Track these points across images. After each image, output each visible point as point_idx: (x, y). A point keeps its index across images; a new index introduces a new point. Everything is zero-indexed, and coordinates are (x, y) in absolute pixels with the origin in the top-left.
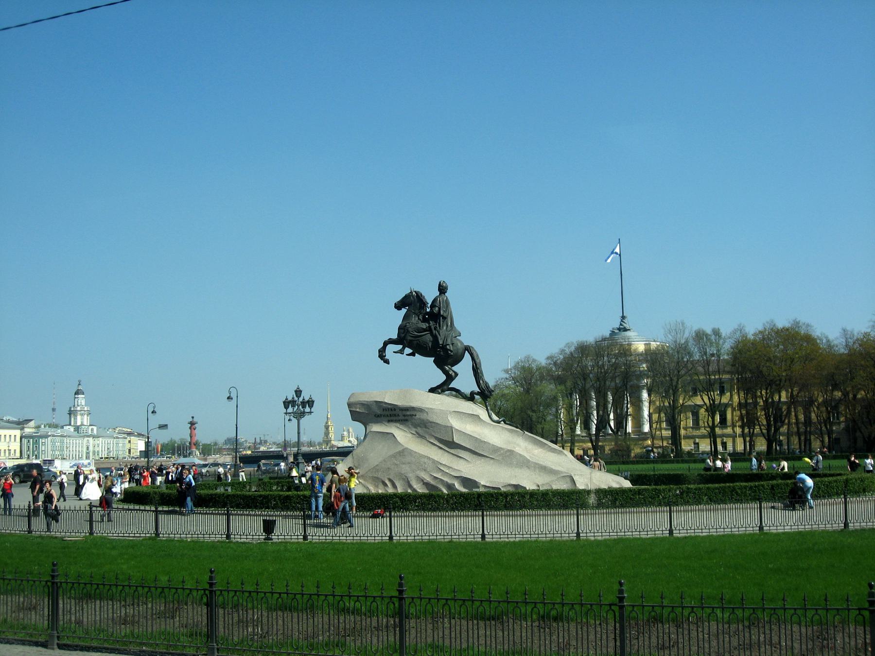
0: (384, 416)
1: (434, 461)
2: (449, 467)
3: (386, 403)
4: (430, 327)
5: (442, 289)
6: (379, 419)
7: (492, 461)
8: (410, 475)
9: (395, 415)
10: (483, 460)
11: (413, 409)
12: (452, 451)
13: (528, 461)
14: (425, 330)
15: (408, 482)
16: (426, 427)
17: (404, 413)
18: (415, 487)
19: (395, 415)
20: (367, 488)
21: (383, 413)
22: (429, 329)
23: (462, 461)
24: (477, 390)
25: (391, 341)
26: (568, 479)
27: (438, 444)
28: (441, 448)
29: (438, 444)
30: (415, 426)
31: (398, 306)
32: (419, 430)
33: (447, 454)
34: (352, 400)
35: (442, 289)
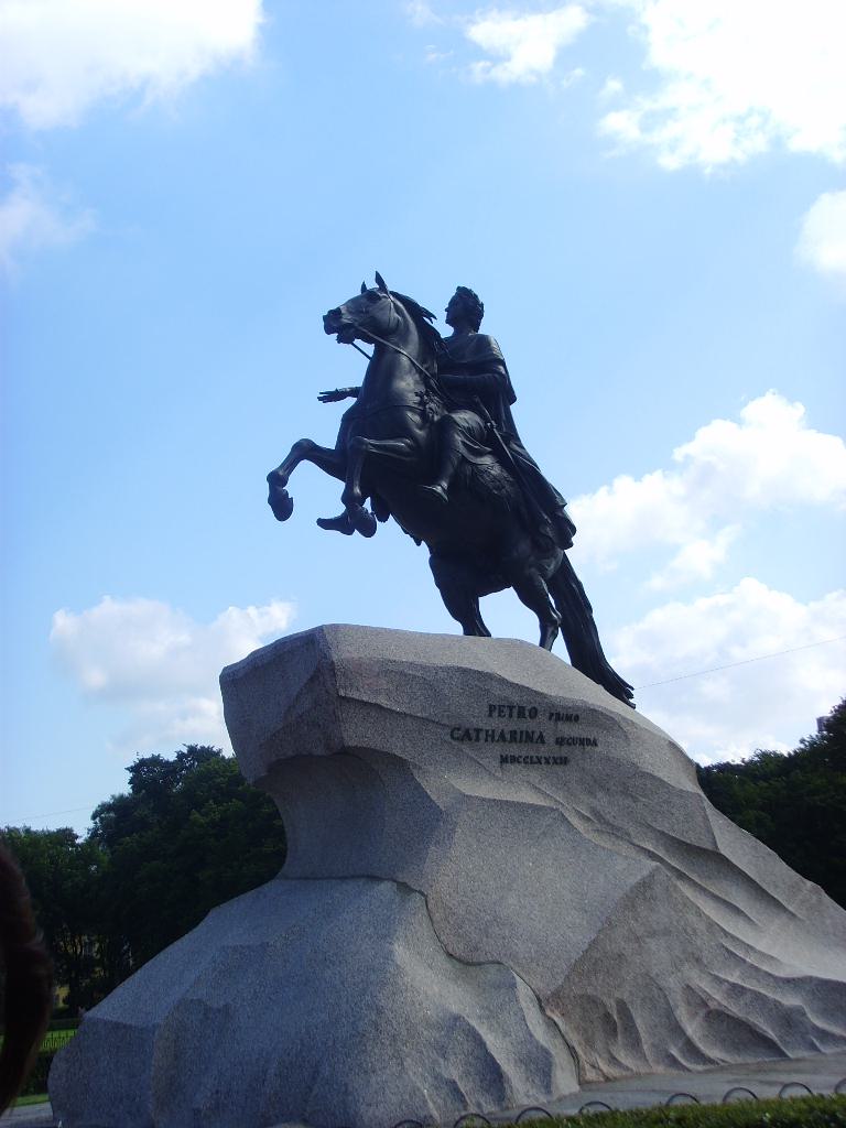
1: (711, 925)
3: (503, 681)
4: (490, 431)
5: (466, 308)
6: (466, 748)
9: (528, 737)
15: (669, 1012)
16: (625, 792)
17: (567, 730)
19: (528, 737)
20: (572, 1050)
21: (497, 724)
23: (741, 923)
25: (305, 451)
28: (681, 876)
31: (340, 325)
32: (602, 801)
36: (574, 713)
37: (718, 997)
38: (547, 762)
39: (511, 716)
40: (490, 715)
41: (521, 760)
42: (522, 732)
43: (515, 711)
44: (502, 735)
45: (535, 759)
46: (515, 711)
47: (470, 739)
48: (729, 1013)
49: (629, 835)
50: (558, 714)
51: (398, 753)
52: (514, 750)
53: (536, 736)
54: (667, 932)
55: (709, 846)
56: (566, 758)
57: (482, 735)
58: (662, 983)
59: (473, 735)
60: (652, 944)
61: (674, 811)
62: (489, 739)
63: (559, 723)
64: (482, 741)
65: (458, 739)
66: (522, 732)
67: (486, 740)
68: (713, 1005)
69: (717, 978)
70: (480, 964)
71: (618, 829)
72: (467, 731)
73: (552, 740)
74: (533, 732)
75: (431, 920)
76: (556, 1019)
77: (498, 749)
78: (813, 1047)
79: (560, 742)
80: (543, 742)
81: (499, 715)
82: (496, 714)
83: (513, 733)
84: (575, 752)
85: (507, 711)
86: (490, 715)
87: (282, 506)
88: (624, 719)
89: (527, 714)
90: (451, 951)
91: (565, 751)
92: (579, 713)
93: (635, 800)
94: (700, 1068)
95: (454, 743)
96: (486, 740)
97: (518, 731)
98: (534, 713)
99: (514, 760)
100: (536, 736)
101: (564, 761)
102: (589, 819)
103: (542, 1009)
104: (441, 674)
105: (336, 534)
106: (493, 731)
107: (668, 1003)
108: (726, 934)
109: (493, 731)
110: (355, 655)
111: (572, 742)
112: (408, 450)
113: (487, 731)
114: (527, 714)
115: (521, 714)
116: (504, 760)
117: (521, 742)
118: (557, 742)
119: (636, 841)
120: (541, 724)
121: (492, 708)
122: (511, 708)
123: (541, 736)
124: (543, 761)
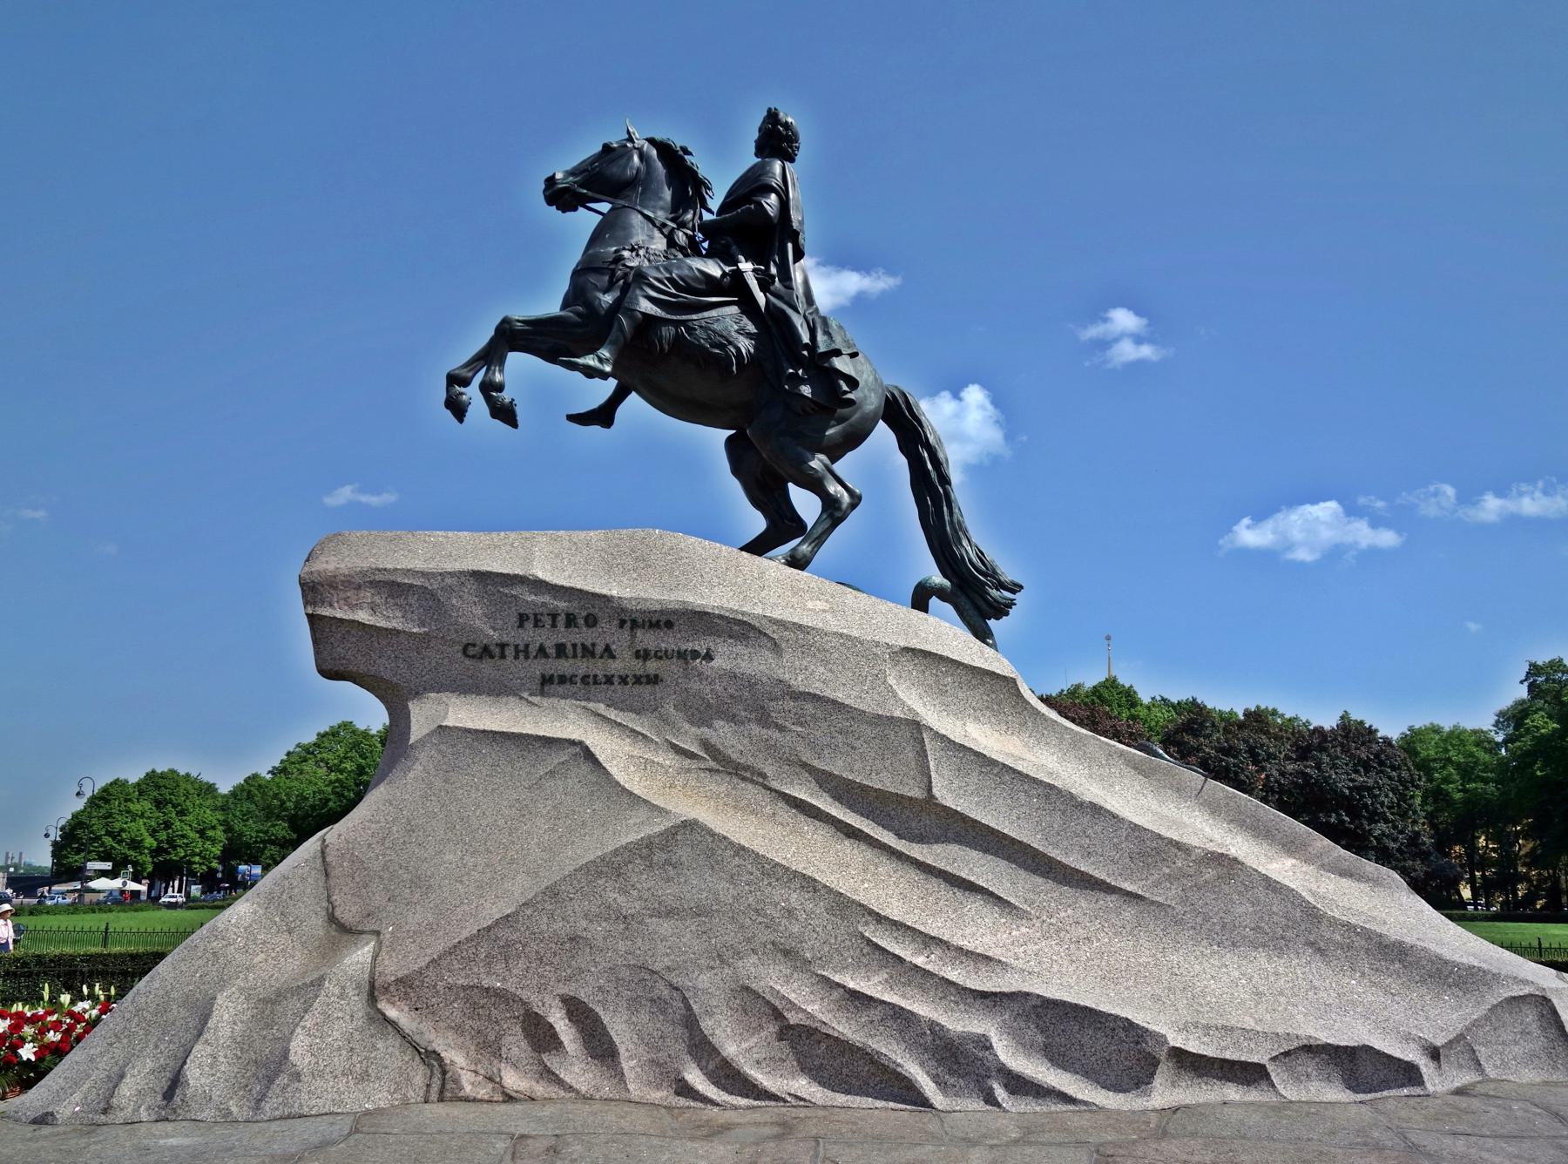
0: (523, 652)
1: (843, 906)
2: (929, 942)
4: (738, 274)
7: (1129, 912)
8: (704, 980)
9: (588, 652)
10: (1085, 902)
11: (703, 621)
12: (916, 851)
13: (1312, 914)
14: (712, 285)
15: (690, 1022)
16: (765, 720)
18: (730, 1049)
19: (588, 652)
20: (430, 1057)
21: (530, 635)
22: (735, 287)
23: (974, 905)
24: (938, 579)
26: (1530, 1016)
27: (836, 811)
29: (836, 811)
30: (701, 713)
33: (886, 866)
34: (329, 564)
35: (776, 140)
36: (664, 618)
37: (812, 1006)
38: (623, 680)
39: (554, 625)
40: (521, 626)
41: (578, 679)
42: (574, 646)
43: (561, 620)
44: (542, 651)
45: (600, 677)
46: (561, 620)
47: (492, 657)
48: (830, 1032)
49: (764, 776)
50: (634, 622)
51: (387, 675)
52: (564, 666)
53: (599, 649)
54: (700, 912)
55: (916, 793)
56: (656, 676)
57: (510, 652)
58: (677, 980)
59: (497, 651)
60: (665, 927)
61: (857, 744)
62: (521, 656)
63: (639, 633)
64: (510, 658)
65: (473, 657)
66: (574, 646)
67: (516, 657)
68: (793, 1018)
69: (826, 980)
70: (362, 932)
71: (747, 768)
72: (486, 649)
73: (628, 654)
74: (593, 645)
75: (327, 875)
76: (392, 1013)
77: (538, 667)
78: (991, 1099)
79: (643, 655)
80: (613, 657)
81: (536, 626)
82: (529, 625)
83: (561, 650)
84: (669, 669)
85: (548, 621)
86: (521, 626)
87: (457, 408)
88: (781, 624)
89: (581, 622)
90: (338, 913)
91: (652, 666)
92: (673, 618)
93: (781, 729)
94: (743, 1102)
95: (467, 662)
96: (516, 657)
97: (569, 647)
98: (591, 621)
99: (563, 680)
100: (599, 649)
101: (654, 680)
102: (692, 756)
103: (372, 998)
104: (449, 581)
105: (596, 429)
106: (527, 646)
107: (689, 1008)
108: (880, 919)
109: (527, 646)
110: (331, 567)
111: (661, 655)
112: (577, 318)
113: (516, 646)
114: (581, 622)
115: (571, 620)
116: (546, 680)
117: (575, 656)
118: (637, 655)
119: (775, 785)
120: (607, 634)
121: (522, 618)
122: (554, 617)
123: (607, 649)
124: (616, 679)
